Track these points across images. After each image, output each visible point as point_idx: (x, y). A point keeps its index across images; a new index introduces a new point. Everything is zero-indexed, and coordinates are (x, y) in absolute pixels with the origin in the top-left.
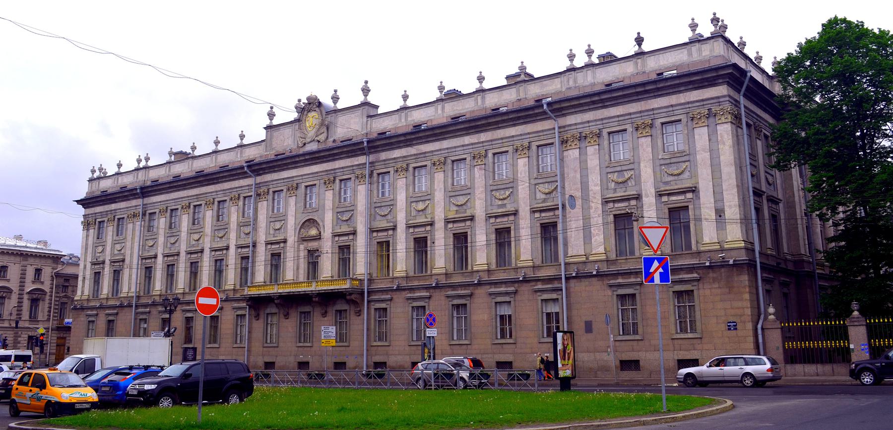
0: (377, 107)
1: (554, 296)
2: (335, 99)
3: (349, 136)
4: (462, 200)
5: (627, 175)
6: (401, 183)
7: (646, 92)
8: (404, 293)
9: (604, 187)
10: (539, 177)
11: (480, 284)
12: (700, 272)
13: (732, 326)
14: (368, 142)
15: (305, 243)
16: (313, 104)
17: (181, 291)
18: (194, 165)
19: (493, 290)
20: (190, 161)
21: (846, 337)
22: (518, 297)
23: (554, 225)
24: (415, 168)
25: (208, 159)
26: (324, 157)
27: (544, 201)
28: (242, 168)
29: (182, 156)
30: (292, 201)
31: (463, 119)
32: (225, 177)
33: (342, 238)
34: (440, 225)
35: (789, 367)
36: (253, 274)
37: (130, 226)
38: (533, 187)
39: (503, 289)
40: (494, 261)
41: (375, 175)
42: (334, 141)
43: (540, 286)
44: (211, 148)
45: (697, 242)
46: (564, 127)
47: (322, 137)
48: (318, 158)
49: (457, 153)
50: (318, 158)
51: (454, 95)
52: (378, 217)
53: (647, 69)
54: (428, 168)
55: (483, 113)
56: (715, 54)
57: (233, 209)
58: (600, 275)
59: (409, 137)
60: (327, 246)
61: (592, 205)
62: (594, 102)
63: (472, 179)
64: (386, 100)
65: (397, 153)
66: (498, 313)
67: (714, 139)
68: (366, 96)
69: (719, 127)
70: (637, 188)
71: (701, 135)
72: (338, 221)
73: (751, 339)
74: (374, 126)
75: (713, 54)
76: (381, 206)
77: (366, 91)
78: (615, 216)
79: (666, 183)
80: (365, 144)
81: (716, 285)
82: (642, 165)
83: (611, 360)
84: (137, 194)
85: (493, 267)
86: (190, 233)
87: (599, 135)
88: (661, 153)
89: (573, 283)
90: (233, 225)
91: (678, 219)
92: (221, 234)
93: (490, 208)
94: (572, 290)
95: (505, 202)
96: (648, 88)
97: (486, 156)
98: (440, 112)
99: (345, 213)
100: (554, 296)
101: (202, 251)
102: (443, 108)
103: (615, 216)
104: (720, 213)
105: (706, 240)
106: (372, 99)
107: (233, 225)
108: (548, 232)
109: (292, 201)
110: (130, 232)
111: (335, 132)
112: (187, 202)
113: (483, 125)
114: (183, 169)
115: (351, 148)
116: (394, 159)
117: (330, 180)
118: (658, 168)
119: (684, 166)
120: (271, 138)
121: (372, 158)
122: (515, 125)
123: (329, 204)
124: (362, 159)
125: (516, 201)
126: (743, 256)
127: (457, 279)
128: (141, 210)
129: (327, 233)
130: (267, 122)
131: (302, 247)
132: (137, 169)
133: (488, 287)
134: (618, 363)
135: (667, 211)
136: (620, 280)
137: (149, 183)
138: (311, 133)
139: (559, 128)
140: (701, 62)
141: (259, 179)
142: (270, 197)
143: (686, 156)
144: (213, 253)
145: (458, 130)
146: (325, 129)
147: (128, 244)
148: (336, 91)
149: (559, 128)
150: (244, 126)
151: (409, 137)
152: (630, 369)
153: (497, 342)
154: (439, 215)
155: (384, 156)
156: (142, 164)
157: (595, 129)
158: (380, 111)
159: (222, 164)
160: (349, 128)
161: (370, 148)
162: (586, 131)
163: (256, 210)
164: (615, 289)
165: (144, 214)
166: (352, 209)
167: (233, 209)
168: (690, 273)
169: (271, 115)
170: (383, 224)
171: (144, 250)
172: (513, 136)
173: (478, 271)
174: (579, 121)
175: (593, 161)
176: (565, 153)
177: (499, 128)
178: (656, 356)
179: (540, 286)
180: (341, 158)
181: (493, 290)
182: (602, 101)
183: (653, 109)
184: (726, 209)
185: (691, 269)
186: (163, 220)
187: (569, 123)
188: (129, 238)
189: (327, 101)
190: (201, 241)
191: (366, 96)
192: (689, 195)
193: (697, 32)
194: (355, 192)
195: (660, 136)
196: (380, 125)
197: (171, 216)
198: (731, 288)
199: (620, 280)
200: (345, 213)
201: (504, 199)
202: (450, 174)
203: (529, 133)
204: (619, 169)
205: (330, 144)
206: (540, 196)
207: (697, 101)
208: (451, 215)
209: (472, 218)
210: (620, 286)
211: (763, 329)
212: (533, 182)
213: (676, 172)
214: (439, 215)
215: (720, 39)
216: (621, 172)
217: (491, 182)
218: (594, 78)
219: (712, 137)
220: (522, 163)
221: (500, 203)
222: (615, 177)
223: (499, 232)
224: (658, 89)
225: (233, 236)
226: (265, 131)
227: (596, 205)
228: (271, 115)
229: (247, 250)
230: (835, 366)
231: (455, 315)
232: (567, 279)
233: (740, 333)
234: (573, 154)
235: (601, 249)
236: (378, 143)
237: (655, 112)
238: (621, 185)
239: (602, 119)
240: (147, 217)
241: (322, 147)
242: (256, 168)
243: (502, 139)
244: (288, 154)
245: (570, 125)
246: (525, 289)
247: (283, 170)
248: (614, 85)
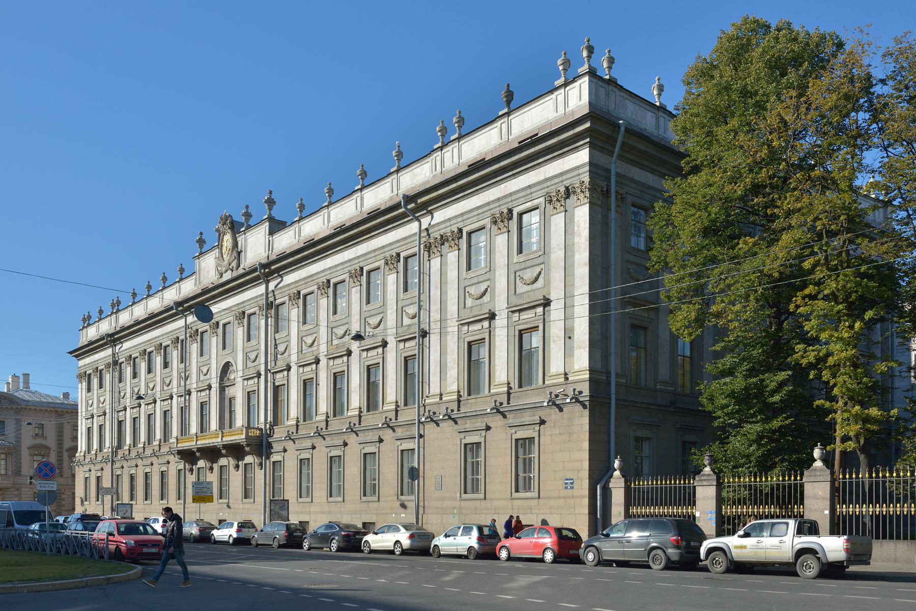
61: (449, 329)
82: (497, 273)
237: (514, 197)
243: (374, 251)
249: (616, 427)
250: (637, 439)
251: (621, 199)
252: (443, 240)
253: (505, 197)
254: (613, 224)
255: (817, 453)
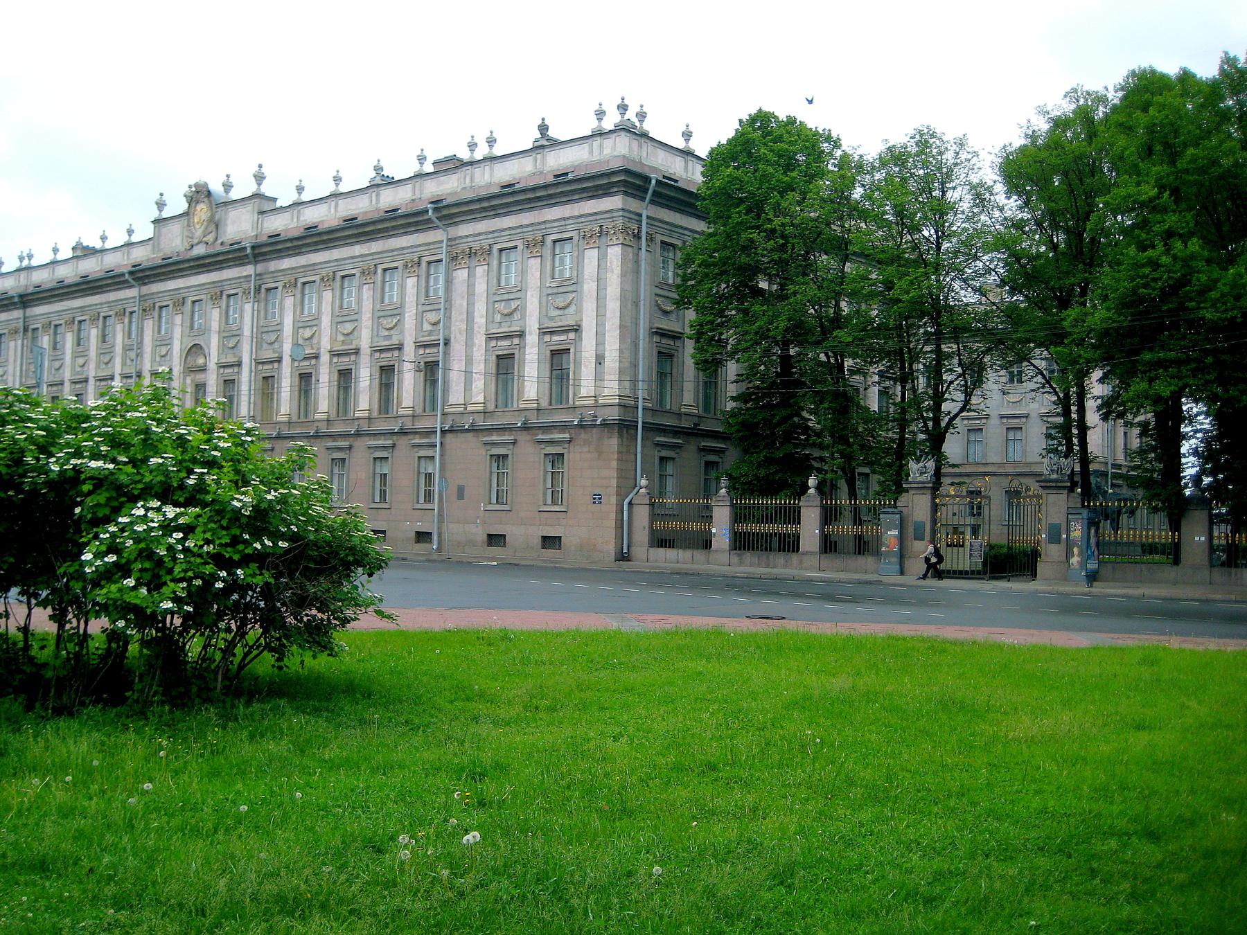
0: (275, 200)
1: (429, 453)
2: (228, 187)
3: (238, 238)
4: (348, 327)
5: (514, 305)
6: (289, 302)
7: (539, 199)
8: (286, 442)
9: (490, 320)
10: (427, 301)
11: (358, 434)
12: (572, 431)
13: (597, 500)
14: (253, 248)
15: (193, 375)
16: (199, 194)
17: (285, 419)
18: (80, 268)
19: (372, 443)
20: (99, 256)
21: (709, 518)
22: (396, 453)
23: (436, 363)
24: (304, 284)
25: (118, 254)
26: (210, 264)
27: (430, 333)
28: (123, 275)
29: (82, 252)
30: (178, 319)
31: (570, 177)
32: (107, 285)
33: (556, 338)
34: (325, 358)
35: (652, 550)
36: (446, 391)
37: (12, 344)
38: (420, 316)
39: (381, 442)
40: (376, 406)
41: (262, 291)
42: (222, 244)
43: (417, 441)
44: (328, 188)
45: (575, 395)
46: (455, 239)
47: (210, 238)
48: (204, 265)
49: (347, 267)
50: (204, 265)
51: (384, 182)
52: (265, 346)
53: (547, 168)
54: (400, 270)
55: (375, 216)
56: (615, 154)
57: (119, 327)
58: (473, 430)
59: (295, 243)
60: (212, 380)
62: (485, 209)
63: (359, 300)
64: (281, 191)
65: (286, 263)
66: (422, 470)
67: (603, 266)
68: (259, 185)
69: (609, 250)
70: (399, 337)
71: (591, 256)
72: (223, 348)
73: (613, 516)
74: (265, 225)
75: (617, 151)
76: (267, 332)
77: (259, 178)
78: (498, 356)
79: (551, 318)
80: (249, 251)
81: (585, 449)
83: (480, 533)
84: (15, 303)
85: (375, 414)
86: (75, 357)
87: (489, 252)
88: (549, 280)
89: (449, 436)
90: (118, 349)
91: (559, 362)
92: (107, 358)
93: (376, 339)
94: (448, 447)
95: (392, 332)
96: (539, 194)
97: (375, 272)
98: (333, 211)
99: (231, 336)
100: (429, 453)
101: (86, 381)
102: (601, 146)
103: (498, 356)
104: (600, 360)
105: (584, 392)
106: (267, 189)
107: (118, 349)
108: (430, 370)
109: (178, 319)
110: (11, 353)
111: (225, 232)
112: (371, 264)
113: (373, 232)
114: (90, 267)
115: (236, 255)
116: (283, 270)
117: (218, 294)
118: (544, 299)
119: (570, 296)
120: (159, 237)
121: (260, 268)
122: (406, 233)
123: (367, 305)
124: (249, 270)
125: (402, 332)
126: (614, 415)
127: (338, 428)
128: (21, 324)
129: (212, 365)
130: (155, 214)
131: (189, 380)
132: (19, 270)
133: (367, 438)
134: (485, 537)
135: (548, 353)
136: (495, 438)
137: (31, 290)
138: (199, 232)
139: (449, 240)
140: (600, 163)
141: (146, 290)
142: (156, 314)
143: (571, 286)
144: (222, 371)
145: (394, 228)
146: (213, 227)
147: (11, 368)
148: (228, 176)
149: (449, 240)
150: (119, 220)
151: (295, 243)
152: (497, 545)
153: (419, 506)
154: (325, 344)
155: (274, 265)
156: (25, 263)
157: (485, 243)
158: (278, 204)
159: (107, 268)
160: (240, 227)
161: (255, 256)
162: (476, 246)
163: (449, 282)
164: (488, 447)
165: (26, 330)
166: (237, 335)
167: (119, 327)
168: (557, 432)
169: (161, 205)
170: (268, 354)
171: (259, 346)
172: (403, 248)
173: (358, 419)
174: (526, 222)
175: (481, 287)
176: (455, 274)
177: (390, 236)
178: (523, 534)
179: (417, 441)
180: (229, 267)
181: (372, 443)
182: (493, 208)
183: (545, 222)
184: (607, 354)
185: (564, 427)
186: (46, 339)
187: (461, 234)
188: (11, 359)
189: (216, 187)
190: (315, 340)
191: (259, 185)
192: (572, 335)
193: (626, 117)
194: (402, 287)
195: (550, 258)
196: (277, 224)
197: (55, 334)
198: (600, 453)
199: (495, 438)
200: (231, 336)
201: (391, 329)
202: (338, 294)
203: (420, 245)
204: (505, 297)
205: (219, 249)
206: (427, 327)
207: (590, 215)
208: (338, 347)
209: (357, 352)
210: (493, 444)
211: (630, 503)
212: (421, 308)
213: (562, 305)
214: (325, 344)
215: (623, 134)
216: (506, 299)
217: (378, 306)
218: (491, 176)
219: (602, 259)
220: (411, 282)
221: (386, 333)
222: (501, 307)
223: (383, 369)
224: (551, 196)
225: (92, 365)
226: (152, 226)
227: (480, 340)
228: (161, 205)
229: (434, 350)
230: (695, 552)
231: (550, 469)
232: (443, 432)
233: (603, 507)
234: (461, 275)
235: (481, 399)
236: (265, 250)
237: (548, 225)
238: (507, 318)
239: (493, 232)
240: (30, 334)
241: (210, 251)
242: (142, 275)
243: (392, 251)
244: (175, 258)
245: (461, 237)
246: (403, 442)
247: (170, 279)
248: (517, 186)
249: (642, 447)
250: (662, 459)
251: (651, 239)
252: (472, 254)
253: (539, 223)
254: (643, 263)
255: (812, 482)
